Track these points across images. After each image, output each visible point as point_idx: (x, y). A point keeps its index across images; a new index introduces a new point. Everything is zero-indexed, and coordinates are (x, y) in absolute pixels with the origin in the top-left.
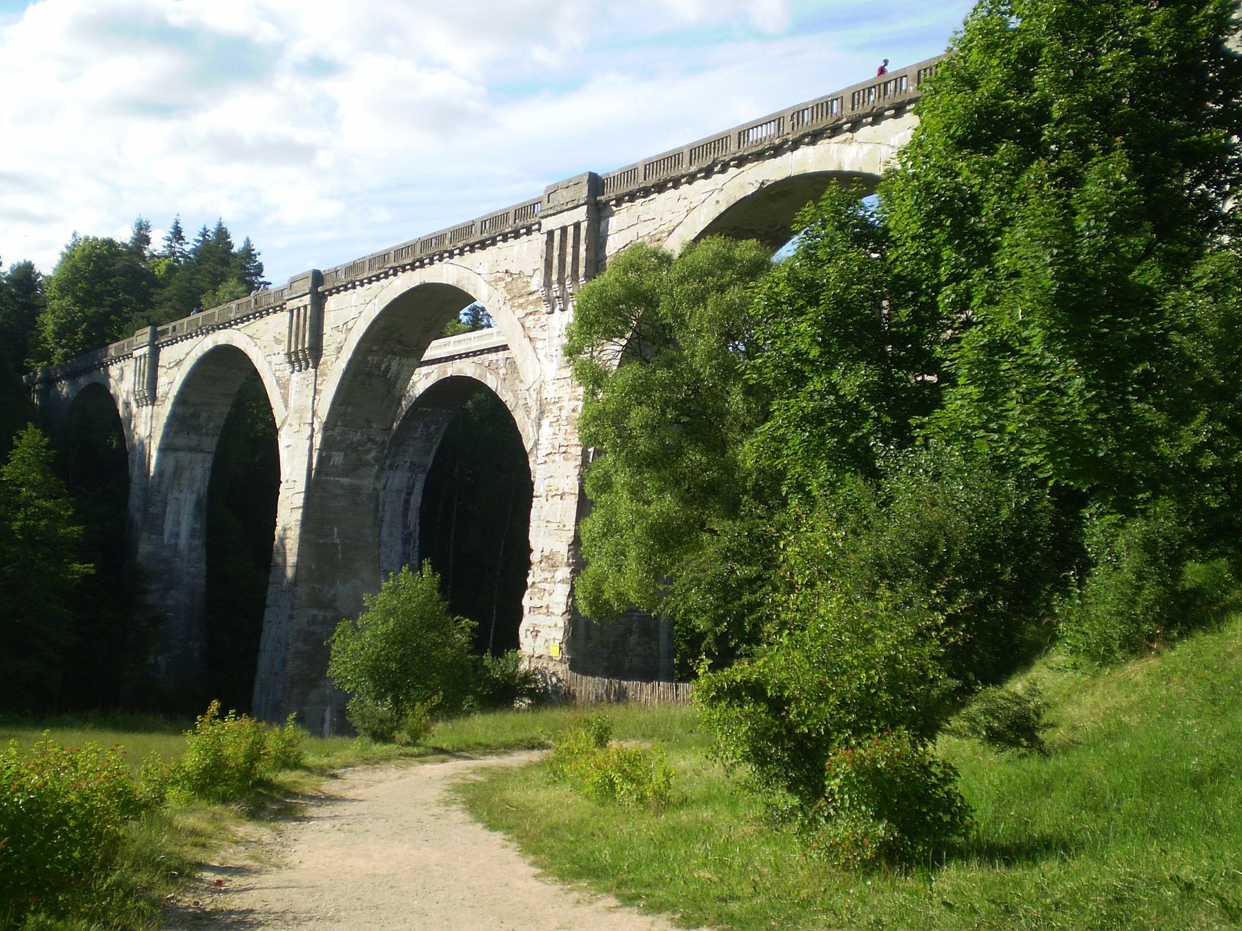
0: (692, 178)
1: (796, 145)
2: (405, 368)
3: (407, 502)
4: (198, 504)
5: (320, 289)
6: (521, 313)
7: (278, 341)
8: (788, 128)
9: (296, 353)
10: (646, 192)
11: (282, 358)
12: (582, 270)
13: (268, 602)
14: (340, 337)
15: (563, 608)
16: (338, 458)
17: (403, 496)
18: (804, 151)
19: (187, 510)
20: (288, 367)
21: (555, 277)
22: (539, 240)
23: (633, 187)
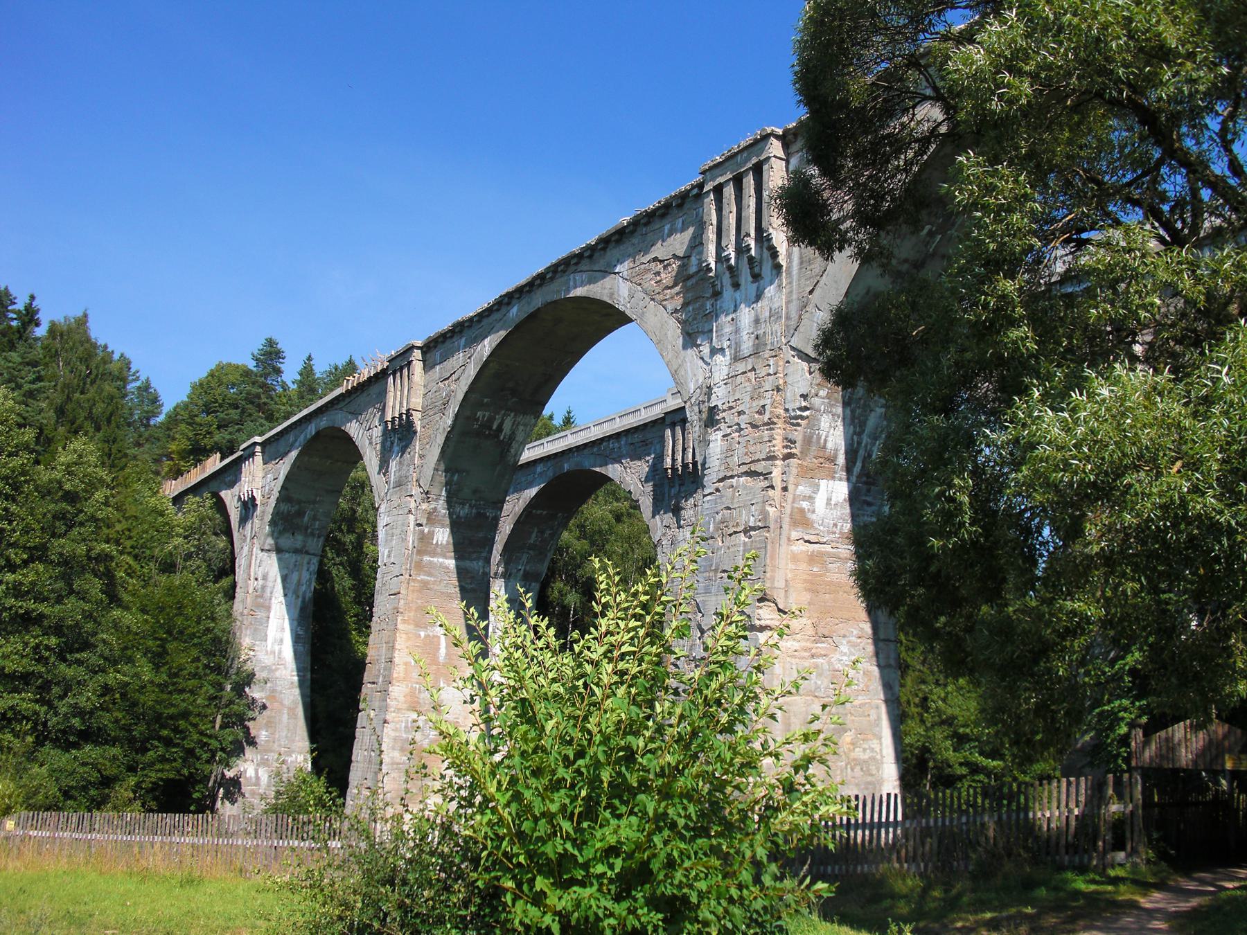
2: (521, 428)
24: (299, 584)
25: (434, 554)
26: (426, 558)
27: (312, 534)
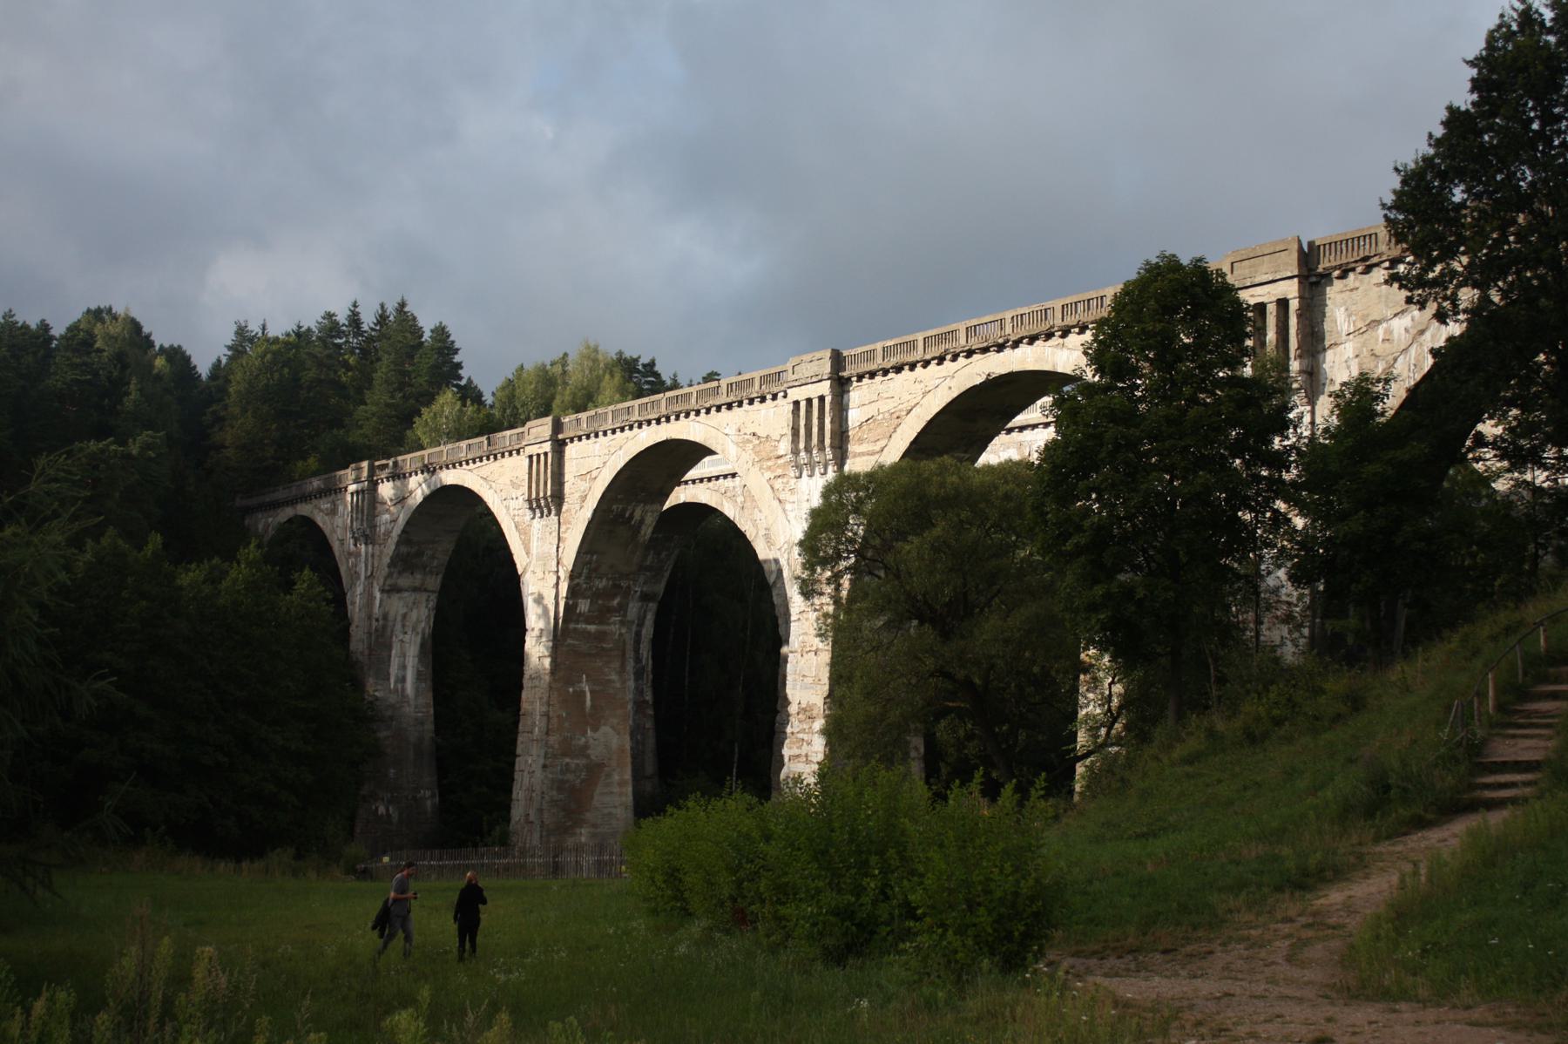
0: (926, 364)
1: (1016, 344)
3: (638, 634)
4: (422, 645)
5: (560, 437)
6: (768, 475)
7: (514, 485)
8: (1008, 330)
9: (538, 500)
10: (886, 372)
11: (521, 503)
12: (827, 441)
13: (519, 751)
14: (583, 485)
15: (820, 757)
16: (583, 606)
17: (634, 628)
18: (1024, 349)
19: (412, 651)
20: (529, 514)
21: (802, 445)
22: (785, 407)
23: (873, 367)
24: (418, 621)
25: (577, 622)
26: (572, 626)
27: (431, 572)
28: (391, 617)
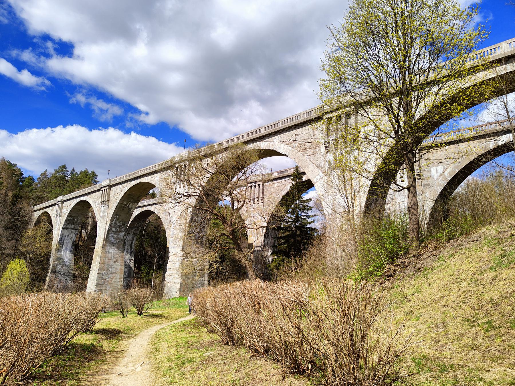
14: (115, 196)
28: (64, 235)
